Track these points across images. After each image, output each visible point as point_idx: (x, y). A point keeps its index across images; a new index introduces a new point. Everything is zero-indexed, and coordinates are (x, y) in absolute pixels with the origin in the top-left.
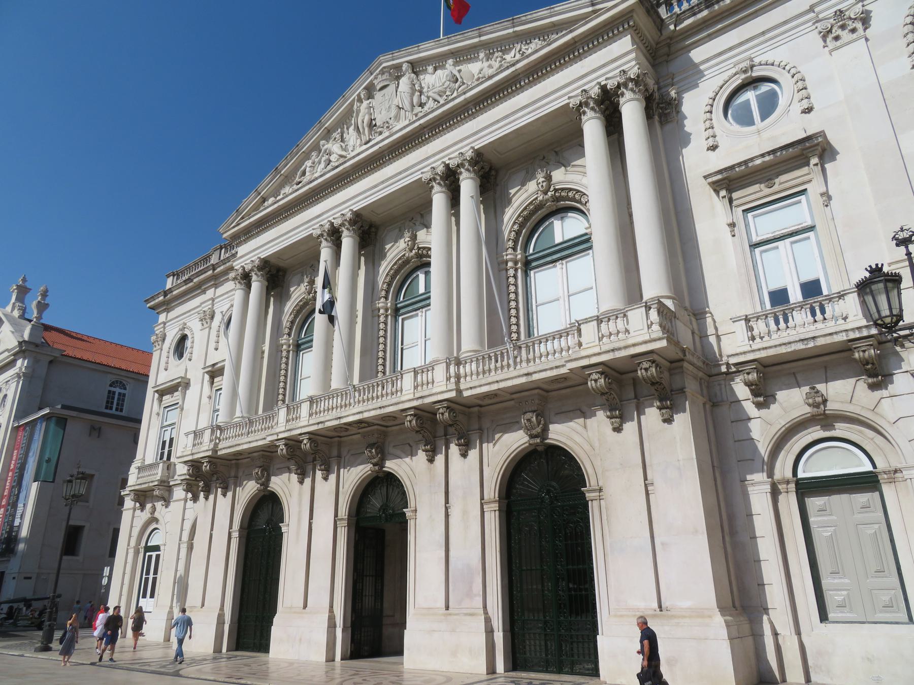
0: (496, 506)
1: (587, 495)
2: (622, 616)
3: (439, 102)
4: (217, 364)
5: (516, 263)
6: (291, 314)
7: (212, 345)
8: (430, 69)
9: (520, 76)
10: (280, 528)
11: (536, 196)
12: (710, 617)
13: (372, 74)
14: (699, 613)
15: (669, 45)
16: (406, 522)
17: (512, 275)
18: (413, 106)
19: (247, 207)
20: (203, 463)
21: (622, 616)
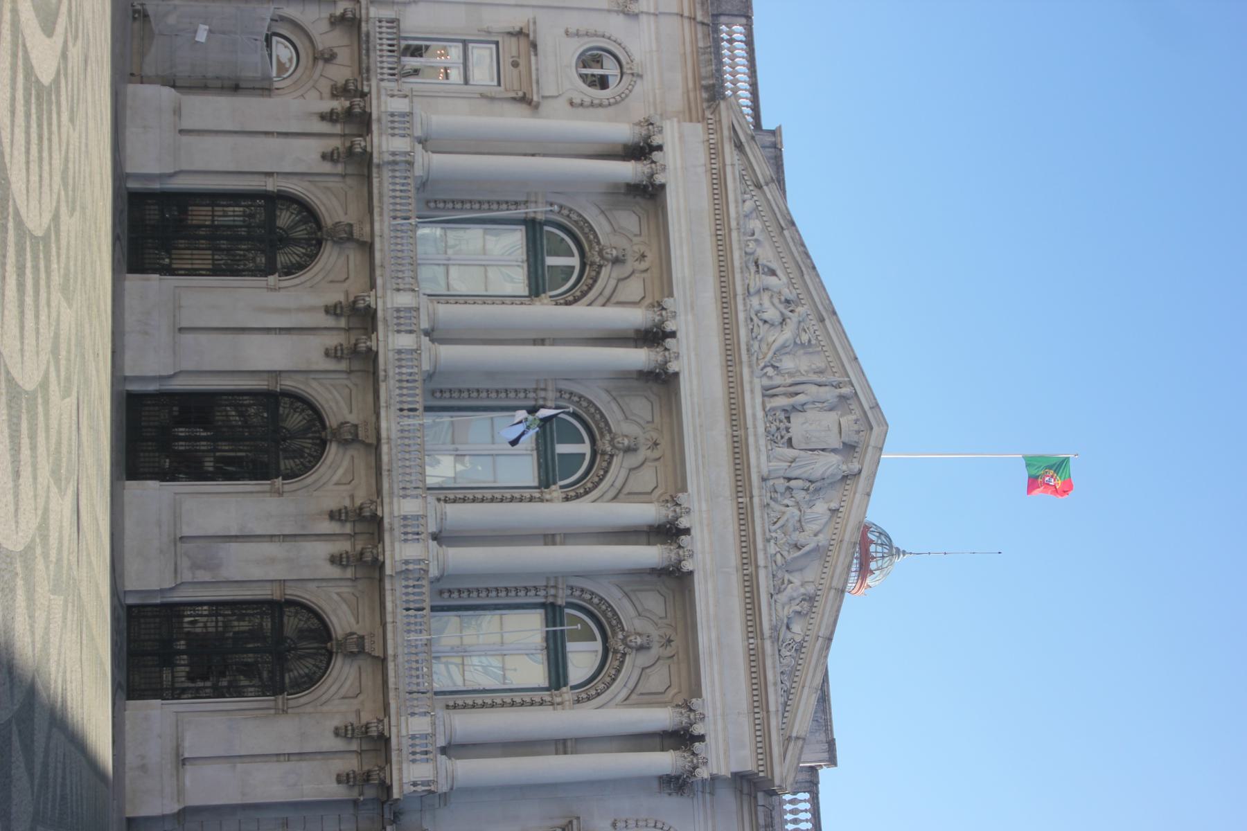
0: (277, 596)
1: (281, 697)
2: (177, 726)
3: (775, 523)
4: (536, 55)
5: (555, 596)
6: (580, 215)
7: (575, 21)
8: (834, 505)
9: (759, 641)
10: (272, 274)
11: (626, 629)
12: (178, 801)
13: (871, 408)
14: (180, 792)
15: (750, 795)
16: (269, 480)
17: (538, 593)
18: (789, 479)
19: (754, 156)
20: (365, 141)
21: (177, 726)
